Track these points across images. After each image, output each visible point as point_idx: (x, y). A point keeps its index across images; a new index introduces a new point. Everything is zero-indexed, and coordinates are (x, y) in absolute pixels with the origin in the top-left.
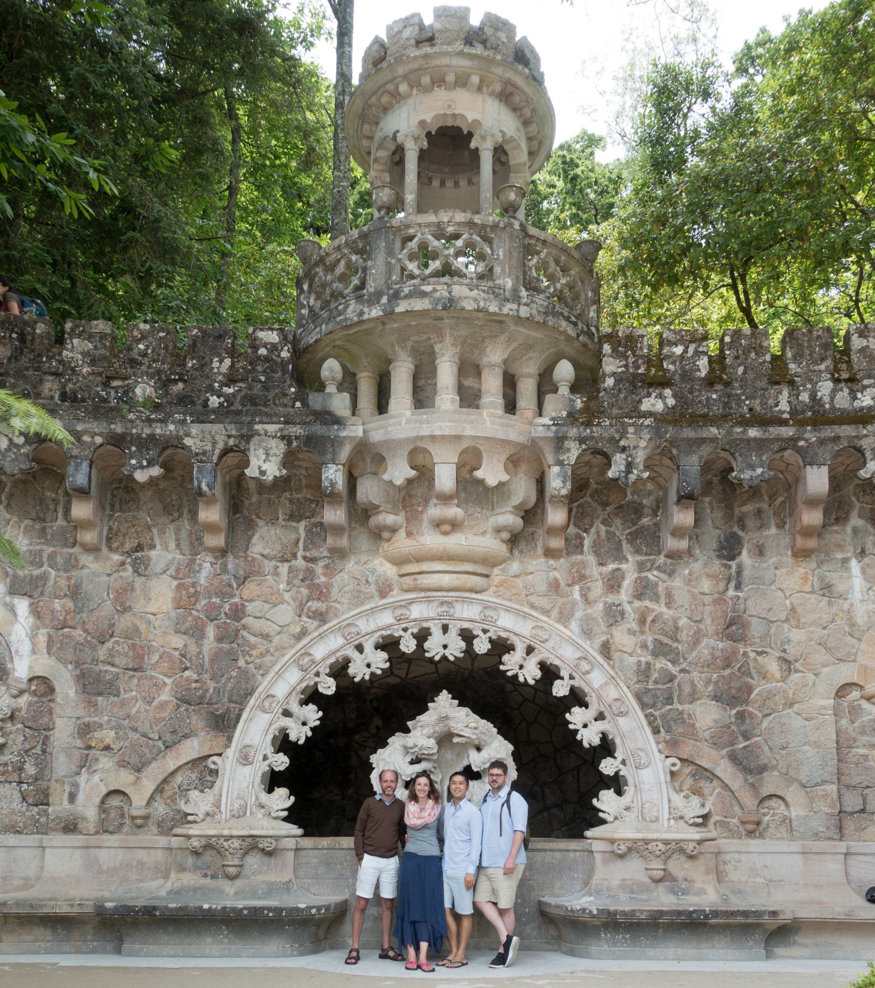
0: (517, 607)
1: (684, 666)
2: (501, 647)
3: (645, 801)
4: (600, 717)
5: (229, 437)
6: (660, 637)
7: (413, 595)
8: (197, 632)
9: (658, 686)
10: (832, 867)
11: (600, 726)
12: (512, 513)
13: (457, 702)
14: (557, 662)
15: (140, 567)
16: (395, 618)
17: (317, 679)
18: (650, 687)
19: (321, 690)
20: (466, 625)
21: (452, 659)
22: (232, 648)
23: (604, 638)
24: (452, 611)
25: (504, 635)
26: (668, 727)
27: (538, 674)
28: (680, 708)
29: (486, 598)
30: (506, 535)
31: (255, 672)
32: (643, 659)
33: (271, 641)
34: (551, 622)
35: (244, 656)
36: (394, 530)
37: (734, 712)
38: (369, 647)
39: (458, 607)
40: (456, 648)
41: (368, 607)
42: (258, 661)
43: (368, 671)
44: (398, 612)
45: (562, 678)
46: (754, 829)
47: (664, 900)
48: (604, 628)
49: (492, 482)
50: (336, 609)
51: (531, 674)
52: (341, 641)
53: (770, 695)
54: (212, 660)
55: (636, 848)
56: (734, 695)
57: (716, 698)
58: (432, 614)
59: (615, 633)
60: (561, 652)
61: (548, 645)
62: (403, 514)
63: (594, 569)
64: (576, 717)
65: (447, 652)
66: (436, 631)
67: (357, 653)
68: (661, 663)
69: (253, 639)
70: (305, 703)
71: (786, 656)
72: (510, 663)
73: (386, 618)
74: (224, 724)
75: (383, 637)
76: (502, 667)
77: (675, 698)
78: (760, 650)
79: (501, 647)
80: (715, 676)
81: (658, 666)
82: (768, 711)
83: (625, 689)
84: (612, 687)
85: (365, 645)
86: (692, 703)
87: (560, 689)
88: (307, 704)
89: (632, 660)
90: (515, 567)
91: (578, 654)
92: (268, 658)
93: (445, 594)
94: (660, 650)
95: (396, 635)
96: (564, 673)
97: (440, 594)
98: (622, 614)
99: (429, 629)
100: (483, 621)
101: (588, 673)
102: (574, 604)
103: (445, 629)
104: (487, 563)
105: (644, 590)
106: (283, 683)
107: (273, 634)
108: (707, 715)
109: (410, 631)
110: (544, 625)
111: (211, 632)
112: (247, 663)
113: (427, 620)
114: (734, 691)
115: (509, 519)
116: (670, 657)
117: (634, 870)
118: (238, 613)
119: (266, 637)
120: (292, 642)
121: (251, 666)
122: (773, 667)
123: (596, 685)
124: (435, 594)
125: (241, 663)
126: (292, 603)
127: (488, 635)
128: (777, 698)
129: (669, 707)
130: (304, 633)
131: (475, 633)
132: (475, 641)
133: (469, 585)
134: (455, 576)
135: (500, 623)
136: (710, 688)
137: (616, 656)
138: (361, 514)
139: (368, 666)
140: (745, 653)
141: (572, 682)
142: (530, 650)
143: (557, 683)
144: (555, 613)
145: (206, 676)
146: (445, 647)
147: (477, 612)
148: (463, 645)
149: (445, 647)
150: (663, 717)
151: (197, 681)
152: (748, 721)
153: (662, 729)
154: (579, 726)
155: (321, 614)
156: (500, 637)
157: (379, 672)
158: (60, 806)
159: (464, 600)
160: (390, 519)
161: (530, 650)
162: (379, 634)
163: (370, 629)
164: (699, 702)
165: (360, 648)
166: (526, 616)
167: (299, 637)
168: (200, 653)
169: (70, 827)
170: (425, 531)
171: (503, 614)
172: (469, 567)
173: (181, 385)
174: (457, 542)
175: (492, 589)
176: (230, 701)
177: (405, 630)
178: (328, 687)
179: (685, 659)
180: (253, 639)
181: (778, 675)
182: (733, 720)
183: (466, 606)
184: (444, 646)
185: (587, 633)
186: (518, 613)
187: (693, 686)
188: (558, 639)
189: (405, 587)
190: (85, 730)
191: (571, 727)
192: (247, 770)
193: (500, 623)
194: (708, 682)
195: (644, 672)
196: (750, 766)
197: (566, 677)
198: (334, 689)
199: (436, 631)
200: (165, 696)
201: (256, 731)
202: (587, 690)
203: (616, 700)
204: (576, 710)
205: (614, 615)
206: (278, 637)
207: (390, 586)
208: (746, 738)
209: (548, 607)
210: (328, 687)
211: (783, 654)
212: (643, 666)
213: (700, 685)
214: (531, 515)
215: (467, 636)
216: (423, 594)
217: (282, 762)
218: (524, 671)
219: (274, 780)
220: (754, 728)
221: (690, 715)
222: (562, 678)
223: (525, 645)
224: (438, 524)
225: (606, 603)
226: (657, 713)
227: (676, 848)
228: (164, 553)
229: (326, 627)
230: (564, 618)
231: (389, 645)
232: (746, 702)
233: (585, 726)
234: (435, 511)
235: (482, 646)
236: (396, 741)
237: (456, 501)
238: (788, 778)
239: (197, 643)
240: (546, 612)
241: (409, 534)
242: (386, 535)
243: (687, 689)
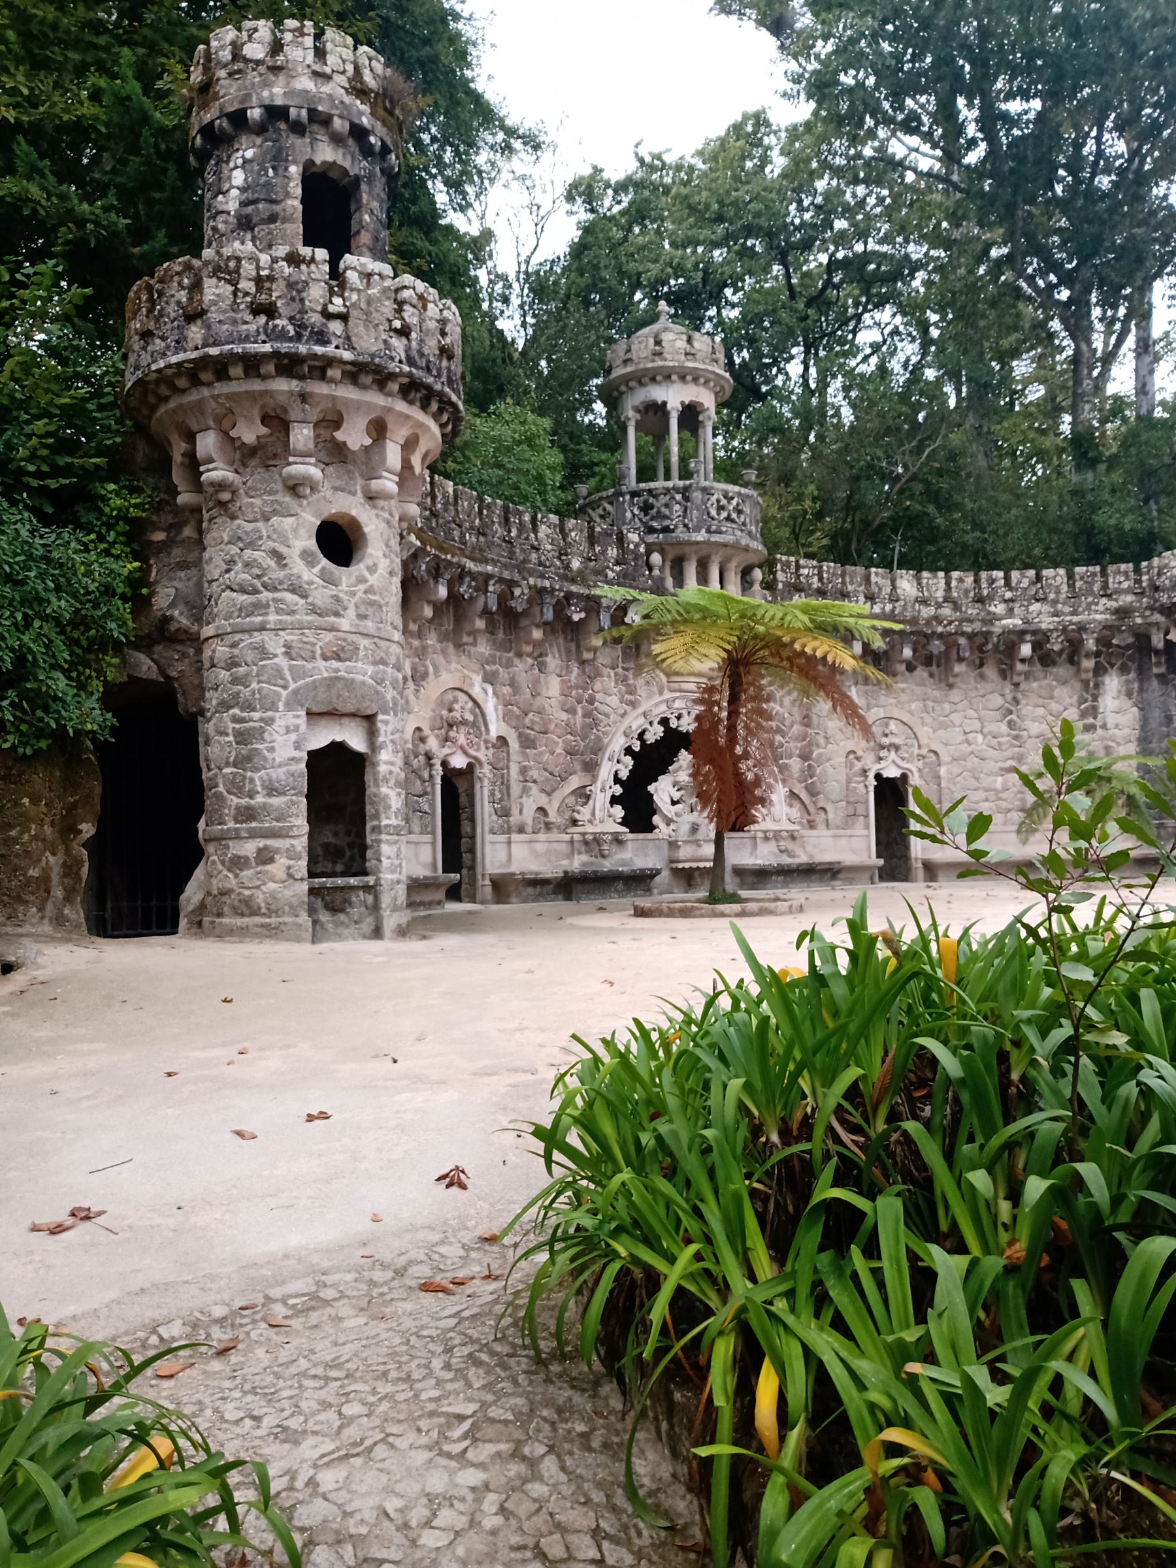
8: (572, 711)
15: (542, 667)
74: (591, 768)
111: (580, 712)
118: (591, 701)
119: (607, 715)
122: (822, 741)
158: (515, 819)
169: (521, 830)
190: (523, 771)
200: (559, 751)
201: (606, 771)
217: (618, 790)
219: (614, 800)
238: (827, 799)
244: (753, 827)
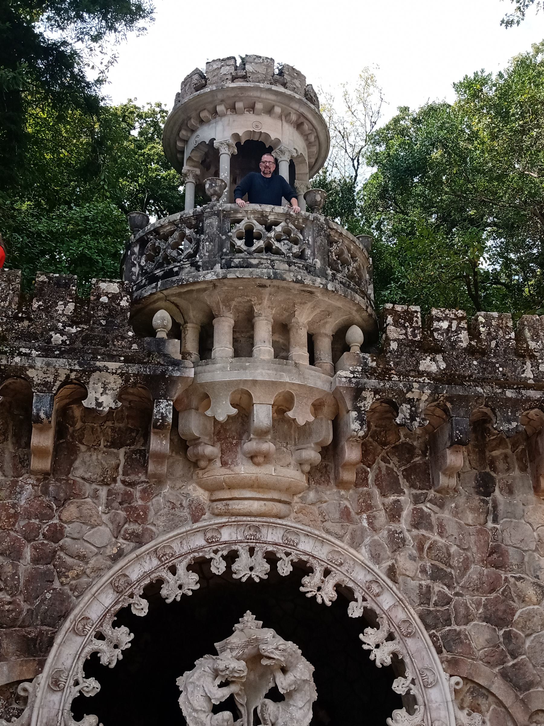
0: (317, 532)
1: (458, 589)
2: (302, 569)
4: (390, 637)
5: (72, 371)
6: (436, 563)
7: (224, 520)
9: (438, 608)
11: (390, 646)
12: (313, 449)
13: (261, 622)
14: (351, 585)
16: (207, 541)
17: (131, 601)
18: (431, 609)
19: (134, 612)
20: (270, 548)
21: (257, 580)
22: (49, 570)
23: (390, 563)
24: (258, 535)
25: (305, 558)
27: (334, 595)
28: (458, 628)
29: (289, 524)
30: (307, 468)
31: (70, 593)
32: (423, 583)
33: (87, 563)
34: (346, 547)
35: (59, 578)
36: (210, 460)
37: (502, 632)
38: (181, 569)
39: (264, 531)
40: (261, 570)
41: (183, 530)
42: (73, 582)
43: (180, 592)
44: (209, 535)
45: (356, 600)
48: (389, 553)
49: (301, 421)
50: (152, 531)
51: (328, 595)
52: (155, 562)
53: (529, 616)
54: (28, 582)
57: (487, 619)
58: (239, 538)
59: (398, 558)
60: (354, 574)
61: (343, 569)
62: (218, 444)
63: (378, 500)
65: (253, 574)
66: (244, 555)
67: (170, 575)
68: (438, 587)
69: (69, 560)
70: (115, 625)
71: (539, 582)
72: (310, 584)
73: (199, 541)
75: (194, 558)
76: (302, 589)
77: (453, 619)
78: (518, 575)
79: (302, 569)
80: (484, 599)
81: (436, 589)
82: (528, 632)
83: (412, 611)
84: (400, 609)
85: (178, 567)
86: (466, 624)
87: (355, 611)
88: (119, 627)
89: (414, 584)
90: (312, 495)
91: (369, 578)
92: (85, 579)
93: (253, 519)
95: (208, 557)
96: (358, 595)
97: (249, 519)
98: (404, 540)
99: (237, 551)
100: (286, 545)
101: (378, 595)
102: (363, 529)
103: (252, 551)
104: (291, 490)
106: (97, 604)
107: (91, 555)
108: (478, 634)
109: (220, 553)
110: (340, 549)
112: (62, 583)
113: (235, 543)
114: (500, 614)
115: (312, 454)
116: (446, 581)
119: (83, 558)
120: (109, 563)
121: (66, 588)
123: (386, 607)
124: (245, 519)
125: (57, 585)
126: (110, 525)
127: (291, 557)
128: (535, 619)
129: (448, 628)
130: (120, 554)
131: (278, 555)
132: (279, 564)
133: (275, 511)
134: (262, 503)
135: (301, 547)
136: (481, 611)
137: (400, 579)
138: (182, 445)
139: (180, 587)
140: (506, 578)
141: (365, 604)
142: (327, 573)
143: (352, 604)
144: (348, 537)
145: (20, 599)
146: (251, 569)
147: (280, 536)
148: (267, 567)
149: (251, 569)
150: (444, 637)
151: (10, 603)
152: (514, 641)
153: (443, 649)
154: (372, 647)
155: (138, 536)
156: (300, 560)
157: (190, 593)
159: (269, 525)
160: (209, 450)
161: (327, 573)
162: (192, 555)
163: (183, 551)
164: (473, 623)
165: (173, 570)
166: (323, 541)
167: (115, 558)
168: (16, 574)
170: (239, 461)
171: (303, 538)
172: (276, 496)
173: (26, 323)
174: (266, 472)
175: (293, 515)
176: (43, 624)
177: (216, 552)
178: (141, 608)
179: (458, 583)
180: (69, 560)
181: (534, 599)
182: (502, 640)
183: (270, 530)
184: (250, 568)
185: (376, 558)
186: (316, 538)
187: (467, 608)
188: (352, 563)
189: (216, 511)
191: (365, 647)
192: (56, 697)
193: (301, 547)
194: (478, 604)
195: (425, 595)
197: (360, 599)
198: (147, 611)
199: (244, 555)
202: (378, 611)
203: (404, 621)
204: (369, 630)
206: (95, 558)
207: (203, 509)
208: (514, 657)
209: (341, 533)
210: (141, 608)
211: (536, 580)
212: (424, 589)
213: (472, 607)
214: (331, 452)
215: (272, 559)
216: (233, 519)
218: (323, 593)
220: (519, 647)
221: (466, 635)
222: (356, 600)
223: (323, 569)
224: (252, 457)
225: (389, 530)
226: (438, 634)
229: (143, 549)
230: (355, 544)
231: (200, 566)
232: (510, 623)
233: (377, 646)
234: (250, 446)
235: (285, 569)
236: (204, 664)
237: (269, 437)
239: (13, 564)
240: (340, 538)
241: (224, 464)
242: (202, 464)
243: (462, 611)
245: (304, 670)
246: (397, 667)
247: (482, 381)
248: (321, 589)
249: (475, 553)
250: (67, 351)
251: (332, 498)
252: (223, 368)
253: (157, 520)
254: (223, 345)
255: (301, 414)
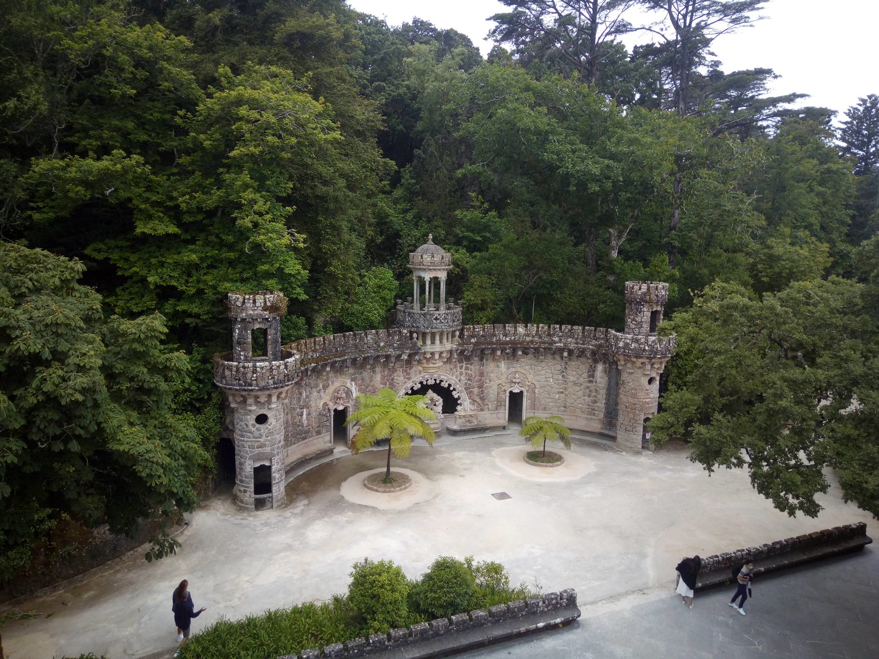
2: (441, 381)
3: (465, 407)
10: (495, 415)
15: (374, 372)
26: (470, 393)
46: (482, 410)
47: (469, 426)
55: (464, 416)
56: (480, 387)
64: (454, 393)
79: (441, 381)
94: (469, 380)
105: (467, 369)
117: (463, 420)
118: (393, 379)
184: (431, 382)
195: (466, 384)
196: (482, 399)
205: (461, 374)
227: (471, 416)
228: (378, 369)
235: (438, 382)
244: (456, 413)
245: (441, 400)
246: (459, 398)
247: (483, 344)
248: (445, 385)
249: (477, 374)
250: (398, 348)
251: (448, 366)
252: (429, 348)
253: (412, 375)
254: (428, 342)
255: (444, 355)
